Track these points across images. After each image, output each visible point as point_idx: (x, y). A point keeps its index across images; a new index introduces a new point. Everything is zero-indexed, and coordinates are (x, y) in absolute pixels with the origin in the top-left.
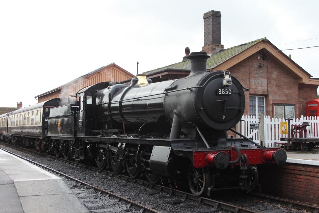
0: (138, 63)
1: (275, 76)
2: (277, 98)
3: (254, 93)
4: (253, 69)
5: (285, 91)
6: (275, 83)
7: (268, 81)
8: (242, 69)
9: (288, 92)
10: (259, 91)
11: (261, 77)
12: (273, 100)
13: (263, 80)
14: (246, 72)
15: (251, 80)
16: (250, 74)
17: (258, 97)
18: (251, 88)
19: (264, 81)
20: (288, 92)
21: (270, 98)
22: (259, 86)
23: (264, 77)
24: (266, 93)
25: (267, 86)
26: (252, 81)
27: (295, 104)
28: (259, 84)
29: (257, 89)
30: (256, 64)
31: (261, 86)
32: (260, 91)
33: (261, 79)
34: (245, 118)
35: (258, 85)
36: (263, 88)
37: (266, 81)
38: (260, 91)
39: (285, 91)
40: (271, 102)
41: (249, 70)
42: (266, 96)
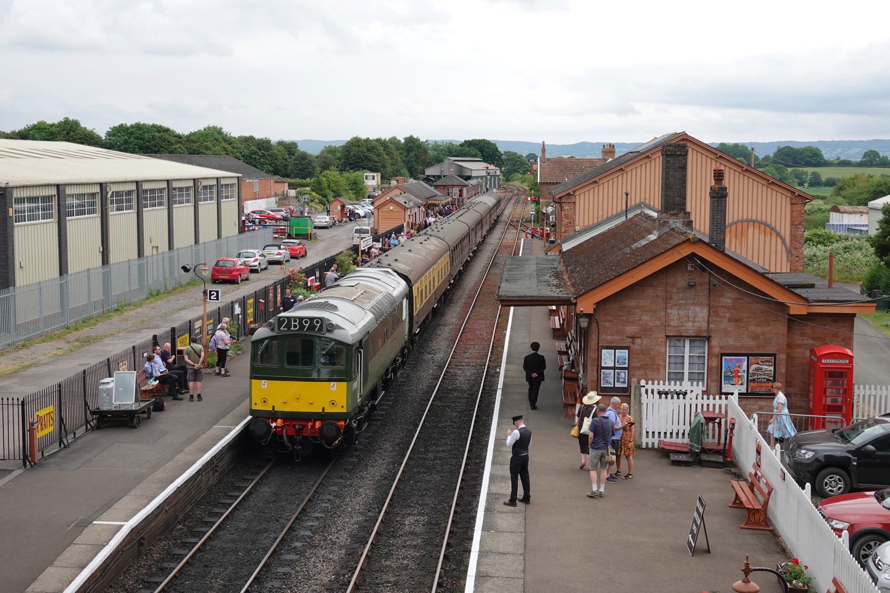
0: (627, 194)
1: (729, 301)
2: (731, 343)
3: (678, 334)
4: (675, 290)
5: (752, 328)
6: (728, 315)
7: (711, 311)
8: (650, 292)
9: (759, 330)
10: (687, 330)
11: (693, 304)
12: (721, 347)
13: (698, 309)
14: (658, 296)
15: (669, 311)
16: (667, 299)
17: (690, 340)
18: (669, 326)
19: (702, 313)
20: (759, 330)
21: (715, 342)
22: (689, 321)
23: (700, 304)
24: (705, 335)
25: (708, 320)
26: (674, 312)
27: (775, 354)
28: (688, 317)
29: (684, 326)
30: (681, 280)
31: (694, 322)
32: (690, 328)
33: (693, 308)
35: (686, 319)
36: (696, 324)
37: (705, 311)
38: (690, 330)
39: (752, 328)
40: (716, 351)
41: (666, 292)
42: (708, 338)
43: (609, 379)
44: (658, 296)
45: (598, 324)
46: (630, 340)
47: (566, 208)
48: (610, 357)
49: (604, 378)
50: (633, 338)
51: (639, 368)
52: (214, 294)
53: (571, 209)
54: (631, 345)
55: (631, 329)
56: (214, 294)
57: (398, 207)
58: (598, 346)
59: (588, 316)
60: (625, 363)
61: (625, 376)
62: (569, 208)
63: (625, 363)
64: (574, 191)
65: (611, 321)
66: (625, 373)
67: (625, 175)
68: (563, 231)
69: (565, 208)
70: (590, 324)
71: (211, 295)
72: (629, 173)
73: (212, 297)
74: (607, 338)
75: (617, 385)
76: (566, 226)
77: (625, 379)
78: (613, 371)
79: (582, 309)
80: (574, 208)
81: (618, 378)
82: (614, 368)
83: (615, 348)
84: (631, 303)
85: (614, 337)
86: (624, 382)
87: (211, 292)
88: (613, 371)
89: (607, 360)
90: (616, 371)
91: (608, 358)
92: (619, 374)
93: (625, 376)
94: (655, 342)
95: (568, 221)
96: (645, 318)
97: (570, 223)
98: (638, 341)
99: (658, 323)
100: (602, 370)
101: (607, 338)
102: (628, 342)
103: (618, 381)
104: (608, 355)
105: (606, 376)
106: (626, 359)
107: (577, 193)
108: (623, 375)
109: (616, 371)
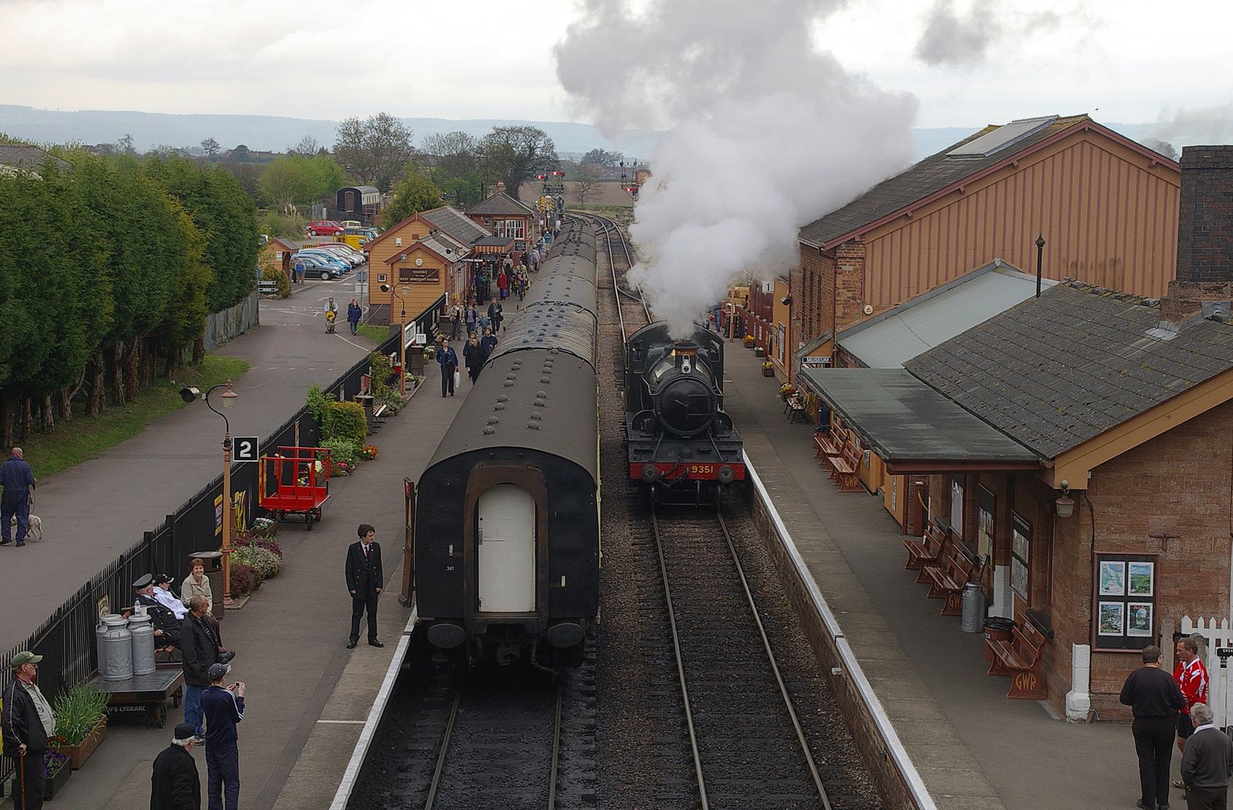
0: (1040, 244)
14: (1215, 456)
34: (1195, 625)
43: (1115, 624)
44: (1215, 456)
45: (1092, 510)
46: (1157, 542)
48: (1117, 576)
49: (1105, 618)
50: (1165, 538)
51: (1178, 599)
52: (246, 447)
53: (855, 270)
54: (1161, 553)
55: (1160, 521)
56: (246, 447)
57: (435, 261)
58: (1093, 554)
59: (1075, 494)
60: (1147, 589)
61: (1148, 614)
62: (851, 268)
63: (1147, 589)
64: (862, 236)
65: (1119, 505)
66: (1147, 608)
67: (964, 202)
68: (839, 314)
70: (1076, 512)
71: (239, 449)
72: (973, 199)
73: (242, 454)
74: (1109, 537)
75: (1131, 633)
76: (846, 304)
77: (1147, 620)
78: (1123, 604)
79: (1065, 482)
80: (863, 270)
81: (1133, 619)
82: (1125, 599)
83: (1127, 558)
84: (1160, 469)
85: (1125, 537)
86: (1145, 627)
87: (238, 441)
88: (1123, 604)
89: (1109, 582)
90: (1129, 604)
91: (1112, 578)
92: (1133, 610)
93: (1148, 614)
94: (1208, 546)
95: (850, 294)
96: (1189, 498)
98: (1175, 545)
99: (1216, 508)
100: (1101, 603)
101: (1109, 537)
102: (1153, 546)
103: (1133, 625)
104: (1113, 573)
105: (1108, 614)
106: (1149, 581)
107: (869, 239)
108: (1143, 612)
109: (1129, 604)
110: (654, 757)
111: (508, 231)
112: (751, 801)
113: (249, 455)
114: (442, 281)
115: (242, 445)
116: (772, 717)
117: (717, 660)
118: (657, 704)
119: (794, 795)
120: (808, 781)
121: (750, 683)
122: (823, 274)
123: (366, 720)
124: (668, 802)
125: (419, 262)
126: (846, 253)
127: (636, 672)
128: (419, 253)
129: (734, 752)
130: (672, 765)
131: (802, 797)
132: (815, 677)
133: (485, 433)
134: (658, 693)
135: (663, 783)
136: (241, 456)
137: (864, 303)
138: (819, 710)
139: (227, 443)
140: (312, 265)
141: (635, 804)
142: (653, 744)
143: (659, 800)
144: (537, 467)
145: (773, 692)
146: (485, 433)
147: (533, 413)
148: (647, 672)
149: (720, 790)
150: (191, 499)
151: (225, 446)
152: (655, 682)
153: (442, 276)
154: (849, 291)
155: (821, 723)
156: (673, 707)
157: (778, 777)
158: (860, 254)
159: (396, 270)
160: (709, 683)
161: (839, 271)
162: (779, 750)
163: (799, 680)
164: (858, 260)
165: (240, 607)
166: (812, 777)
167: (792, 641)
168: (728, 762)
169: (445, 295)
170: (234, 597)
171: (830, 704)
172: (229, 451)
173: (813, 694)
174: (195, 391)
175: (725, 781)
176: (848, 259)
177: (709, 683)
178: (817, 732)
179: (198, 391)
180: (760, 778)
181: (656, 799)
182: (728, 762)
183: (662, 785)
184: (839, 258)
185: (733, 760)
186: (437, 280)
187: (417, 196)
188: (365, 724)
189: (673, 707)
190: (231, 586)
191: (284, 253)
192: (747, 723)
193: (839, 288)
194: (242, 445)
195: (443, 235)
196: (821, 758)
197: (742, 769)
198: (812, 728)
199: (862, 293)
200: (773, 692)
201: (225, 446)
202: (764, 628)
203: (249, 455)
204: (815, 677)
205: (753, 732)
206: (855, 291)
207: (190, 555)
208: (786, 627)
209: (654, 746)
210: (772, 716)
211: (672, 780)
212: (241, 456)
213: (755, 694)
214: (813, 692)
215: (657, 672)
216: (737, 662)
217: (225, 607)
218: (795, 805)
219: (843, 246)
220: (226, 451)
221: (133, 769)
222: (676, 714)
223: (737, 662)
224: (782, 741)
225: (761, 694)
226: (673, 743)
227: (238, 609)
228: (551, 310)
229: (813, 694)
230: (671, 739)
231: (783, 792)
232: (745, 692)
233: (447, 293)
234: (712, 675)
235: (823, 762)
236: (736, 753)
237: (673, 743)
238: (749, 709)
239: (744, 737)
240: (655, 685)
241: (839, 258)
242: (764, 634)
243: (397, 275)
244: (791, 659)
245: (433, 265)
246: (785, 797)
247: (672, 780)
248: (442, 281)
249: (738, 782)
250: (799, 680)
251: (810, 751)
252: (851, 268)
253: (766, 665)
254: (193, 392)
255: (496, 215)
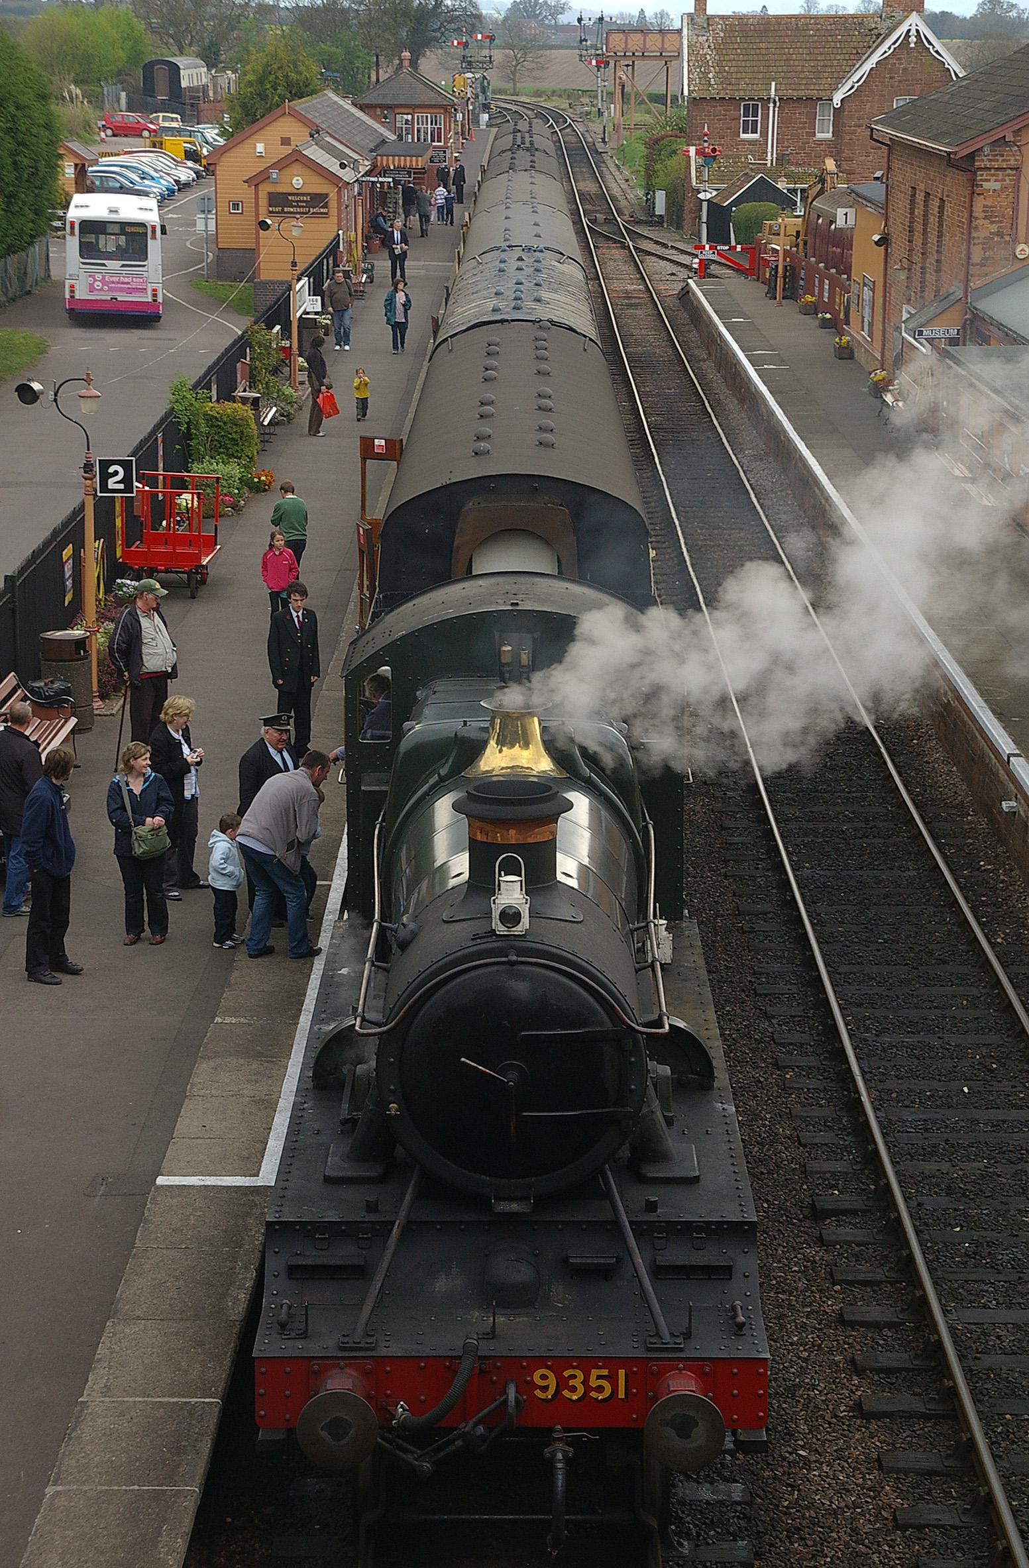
47: (992, 185)
52: (116, 473)
53: (1004, 188)
56: (116, 473)
57: (322, 180)
62: (997, 186)
64: (1017, 132)
68: (976, 258)
69: (986, 185)
71: (105, 476)
73: (112, 483)
87: (105, 464)
97: (999, 234)
110: (744, 932)
111: (419, 131)
112: (898, 997)
113: (121, 486)
114: (333, 211)
115: (111, 470)
116: (911, 875)
117: (817, 791)
118: (736, 855)
119: (961, 988)
120: (980, 967)
121: (872, 824)
122: (947, 196)
123: (332, 880)
124: (775, 998)
125: (298, 182)
126: (990, 160)
127: (698, 808)
128: (297, 168)
129: (863, 926)
130: (772, 945)
131: (974, 991)
132: (969, 815)
133: (476, 454)
134: (736, 839)
135: (763, 971)
136: (110, 487)
137: (1015, 241)
138: (982, 863)
139: (88, 467)
140: (118, 185)
141: (726, 1001)
142: (739, 915)
143: (760, 995)
144: (561, 505)
145: (908, 838)
146: (476, 454)
147: (541, 422)
148: (715, 810)
149: (850, 981)
150: (34, 552)
151: (85, 472)
152: (730, 823)
153: (333, 204)
154: (993, 222)
155: (988, 883)
156: (761, 860)
157: (934, 961)
158: (1012, 162)
159: (263, 195)
160: (811, 825)
161: (978, 190)
162: (931, 922)
163: (946, 820)
164: (1009, 171)
165: (114, 712)
166: (988, 960)
167: (927, 762)
168: (857, 940)
169: (339, 235)
170: (103, 697)
171: (998, 855)
172: (91, 479)
173: (969, 841)
174: (36, 386)
175: (856, 969)
176: (993, 171)
177: (811, 825)
178: (984, 896)
179: (42, 388)
180: (906, 964)
181: (756, 994)
182: (857, 940)
183: (761, 974)
184: (980, 169)
185: (863, 937)
186: (325, 210)
187: (280, 74)
188: (330, 885)
189: (761, 860)
190: (99, 681)
191: (76, 165)
192: (876, 884)
193: (977, 218)
194: (111, 470)
195: (328, 139)
196: (995, 933)
197: (878, 950)
198: (975, 890)
199: (1014, 225)
200: (908, 838)
201: (85, 472)
202: (883, 743)
203: (121, 486)
204: (969, 815)
205: (886, 896)
206: (1001, 222)
207: (41, 635)
208: (915, 741)
209: (740, 918)
210: (912, 873)
211: (776, 967)
212: (110, 487)
213: (881, 840)
214: (969, 838)
215: (730, 809)
216: (848, 793)
217: (96, 712)
218: (965, 1002)
219: (987, 150)
220: (86, 479)
221: (8, 947)
222: (768, 870)
223: (848, 793)
224: (931, 909)
225: (890, 841)
226: (770, 913)
227: (112, 715)
228: (520, 259)
229: (969, 841)
230: (766, 907)
231: (944, 984)
232: (867, 837)
233: (341, 232)
234: (812, 812)
235: (999, 940)
236: (866, 928)
237: (770, 913)
238: (876, 863)
239: (875, 904)
240: (729, 828)
241: (980, 169)
242: (883, 750)
243: (263, 202)
244: (929, 788)
245: (318, 186)
246: (949, 990)
247: (776, 967)
248: (333, 211)
249: (875, 969)
250: (946, 820)
251: (979, 923)
252: (997, 186)
253: (893, 798)
254: (35, 389)
255: (401, 106)
